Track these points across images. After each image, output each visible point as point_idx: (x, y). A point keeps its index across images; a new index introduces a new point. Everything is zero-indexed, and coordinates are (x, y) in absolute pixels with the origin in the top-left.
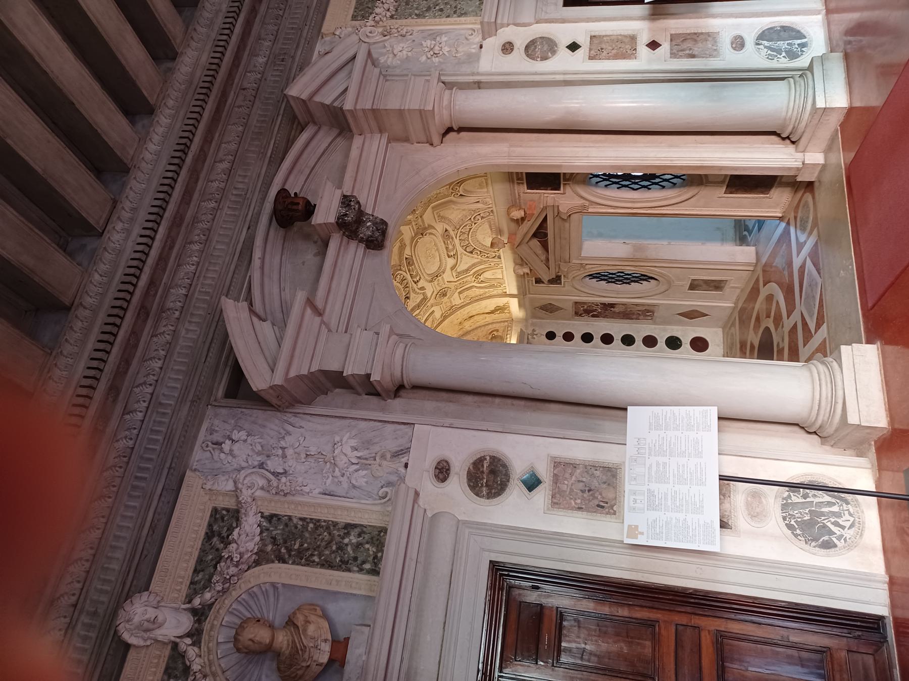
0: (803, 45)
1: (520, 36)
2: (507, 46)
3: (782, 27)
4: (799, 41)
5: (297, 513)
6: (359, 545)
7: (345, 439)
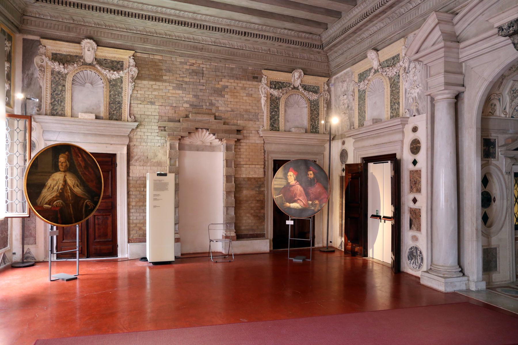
5: (400, 84)
6: (395, 109)
7: (420, 88)
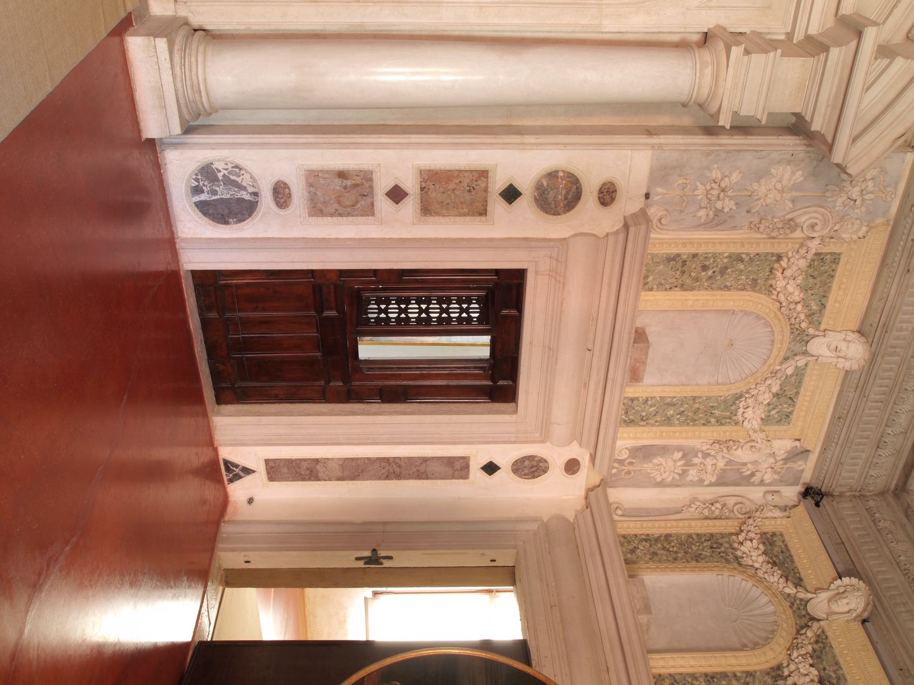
0: (197, 190)
1: (589, 217)
2: (607, 198)
3: (226, 223)
4: (203, 197)
